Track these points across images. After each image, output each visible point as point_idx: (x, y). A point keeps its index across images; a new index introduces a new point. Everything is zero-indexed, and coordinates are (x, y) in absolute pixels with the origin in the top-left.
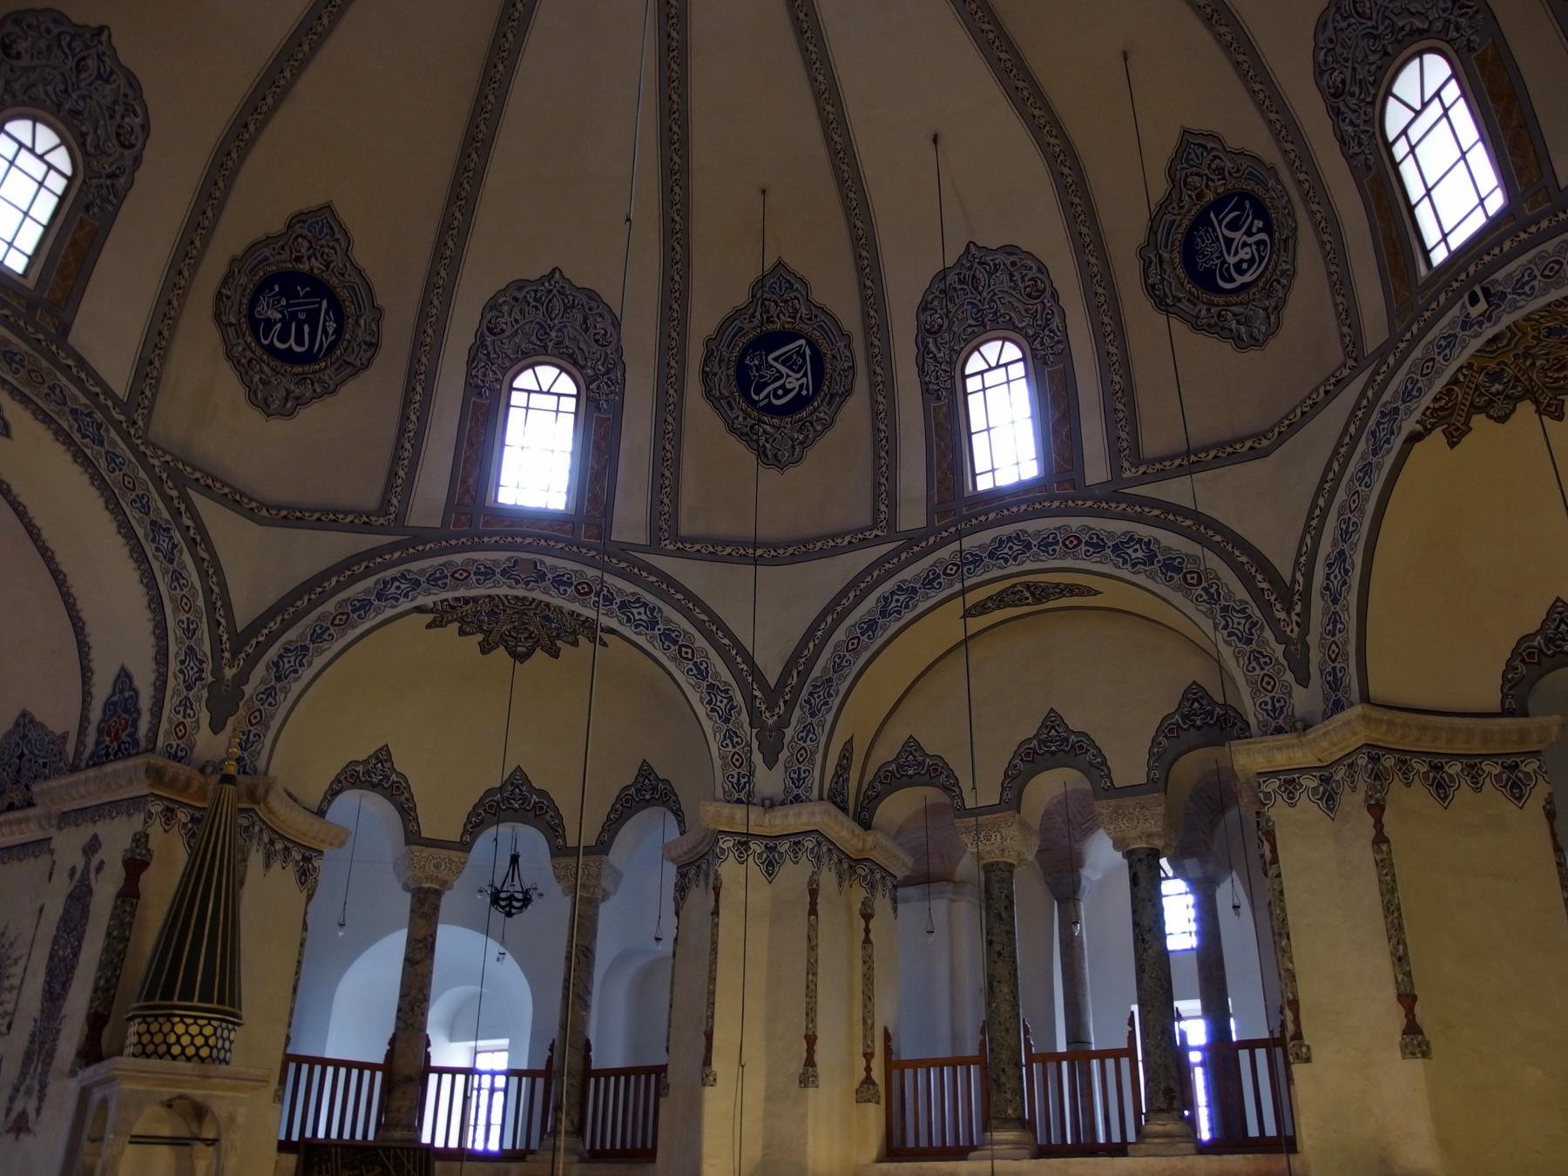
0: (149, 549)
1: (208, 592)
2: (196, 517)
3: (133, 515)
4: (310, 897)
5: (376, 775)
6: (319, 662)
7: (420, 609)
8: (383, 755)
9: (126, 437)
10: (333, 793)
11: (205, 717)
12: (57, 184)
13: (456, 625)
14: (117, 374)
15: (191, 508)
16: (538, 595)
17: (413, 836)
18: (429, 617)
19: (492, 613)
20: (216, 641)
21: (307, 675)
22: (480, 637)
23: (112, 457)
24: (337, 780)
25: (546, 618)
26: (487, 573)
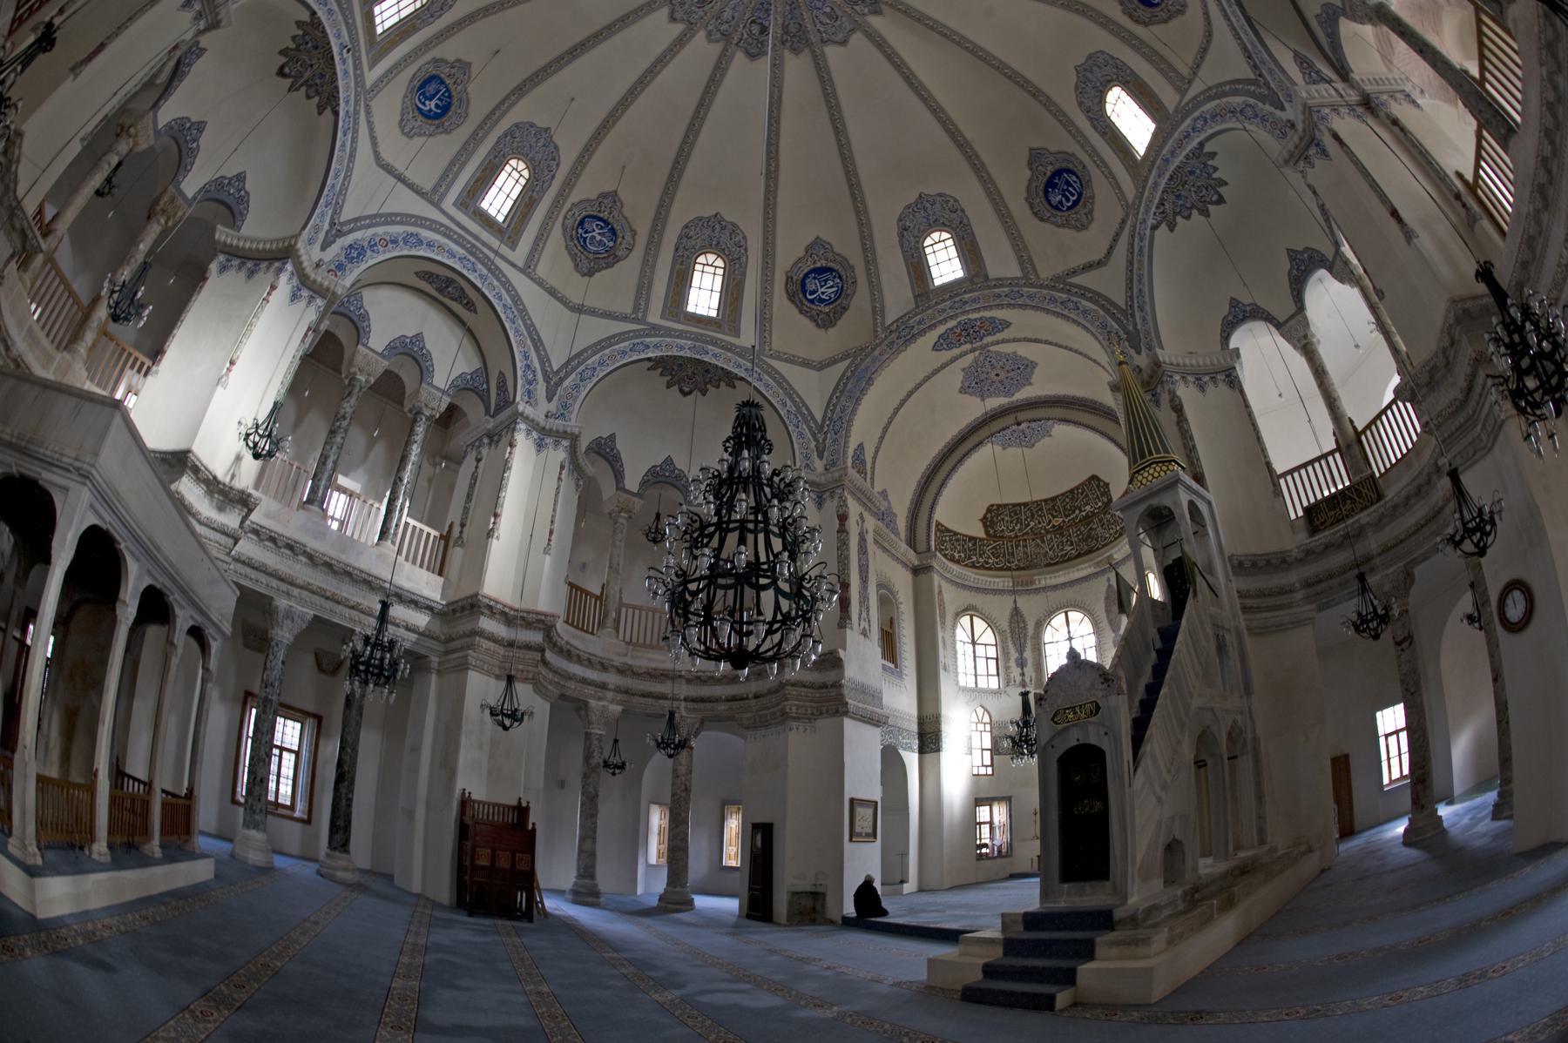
0: (1066, 312)
1: (1102, 307)
2: (1076, 286)
3: (1051, 307)
4: (1242, 391)
5: (1239, 314)
6: (1146, 289)
7: (1154, 228)
8: (1234, 303)
9: (1031, 286)
10: (1226, 339)
11: (1132, 352)
12: (950, 242)
13: (1179, 219)
14: (1015, 271)
15: (1071, 285)
16: (1172, 168)
17: (1279, 326)
18: (1164, 227)
19: (1178, 197)
20: (1117, 320)
21: (1147, 299)
22: (1195, 212)
23: (1030, 297)
24: (1223, 331)
25: (1191, 173)
26: (1156, 184)
